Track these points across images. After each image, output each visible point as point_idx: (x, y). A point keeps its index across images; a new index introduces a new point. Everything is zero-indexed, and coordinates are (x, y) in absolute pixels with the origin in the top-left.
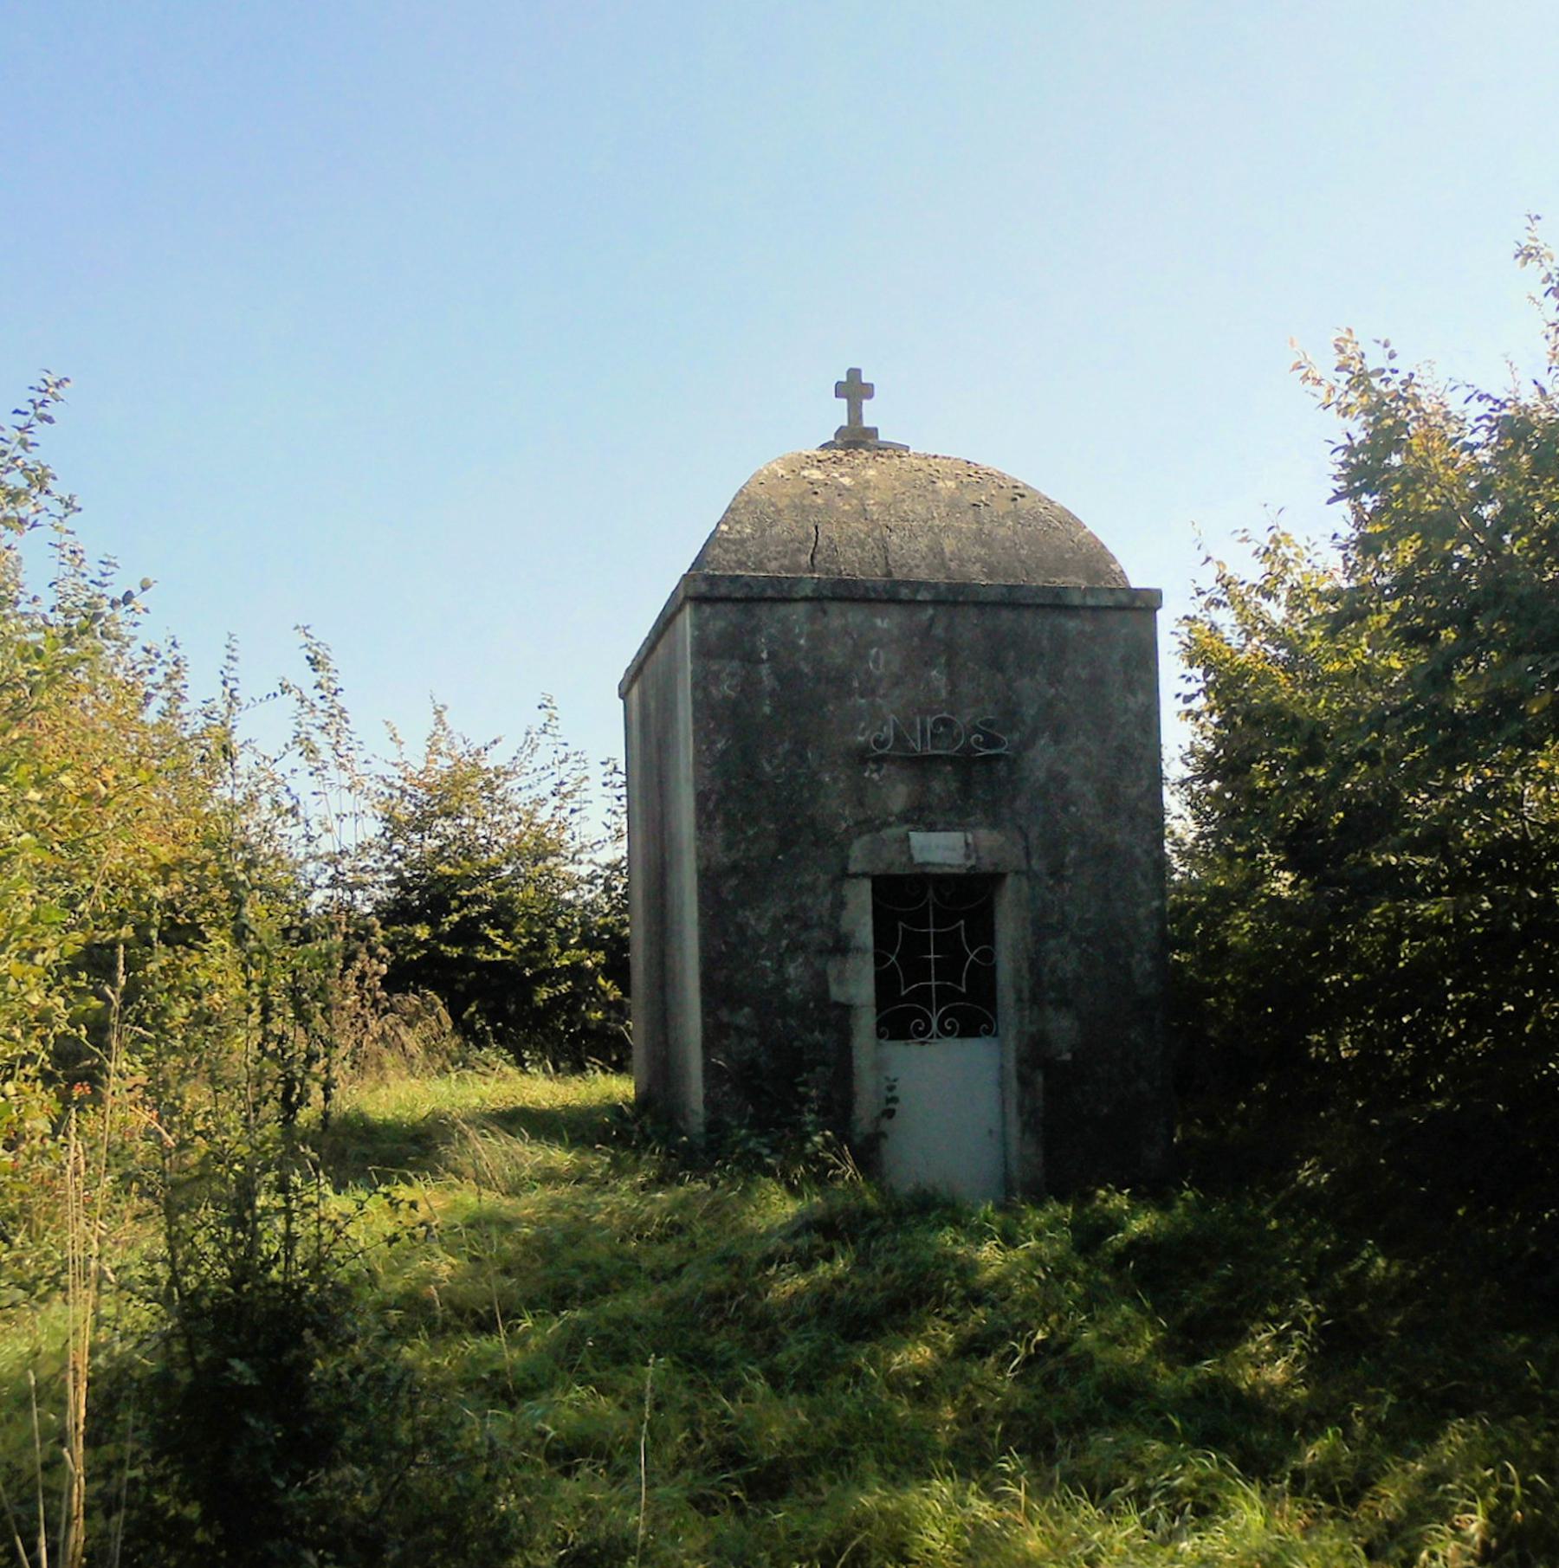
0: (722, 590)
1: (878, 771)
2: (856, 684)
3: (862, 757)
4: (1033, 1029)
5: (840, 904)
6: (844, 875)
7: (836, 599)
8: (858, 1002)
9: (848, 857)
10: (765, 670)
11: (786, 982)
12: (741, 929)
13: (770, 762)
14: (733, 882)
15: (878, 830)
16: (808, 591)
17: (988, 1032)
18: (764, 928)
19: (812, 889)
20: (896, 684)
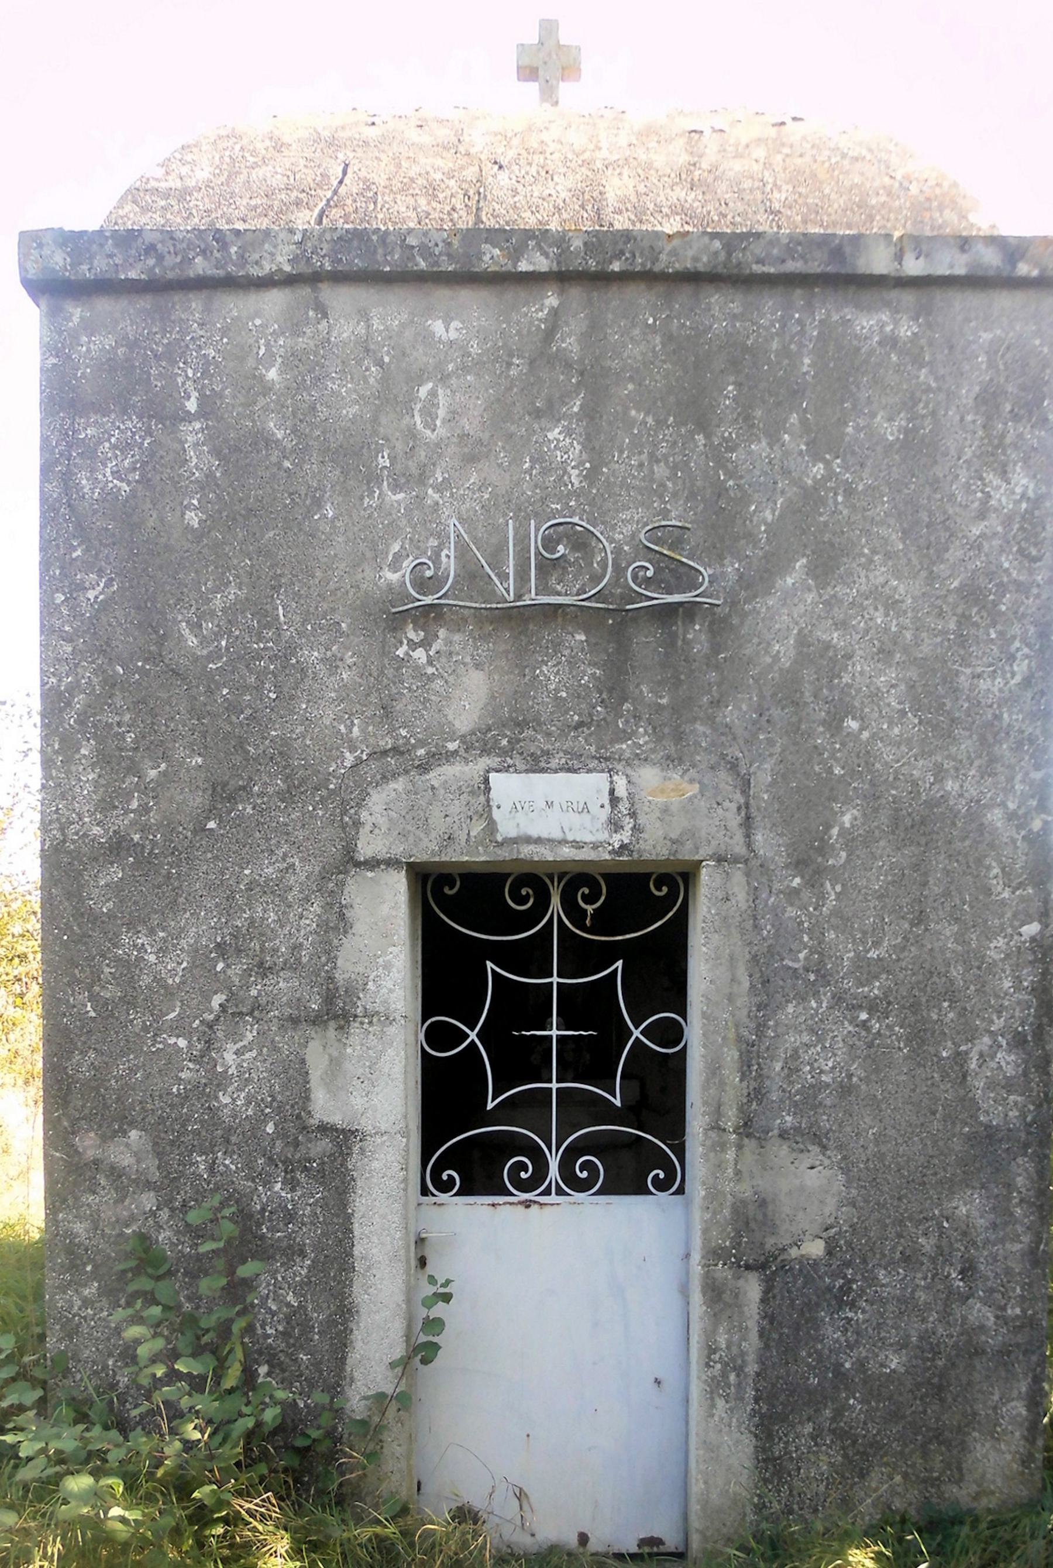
0: (101, 266)
1: (426, 644)
2: (384, 461)
3: (396, 616)
4: (745, 1190)
5: (337, 922)
6: (350, 861)
7: (340, 278)
8: (366, 1124)
9: (357, 824)
10: (192, 433)
11: (221, 1081)
12: (129, 968)
13: (196, 627)
14: (116, 873)
15: (424, 768)
16: (280, 259)
17: (662, 1186)
18: (174, 968)
19: (276, 889)
20: (471, 459)
